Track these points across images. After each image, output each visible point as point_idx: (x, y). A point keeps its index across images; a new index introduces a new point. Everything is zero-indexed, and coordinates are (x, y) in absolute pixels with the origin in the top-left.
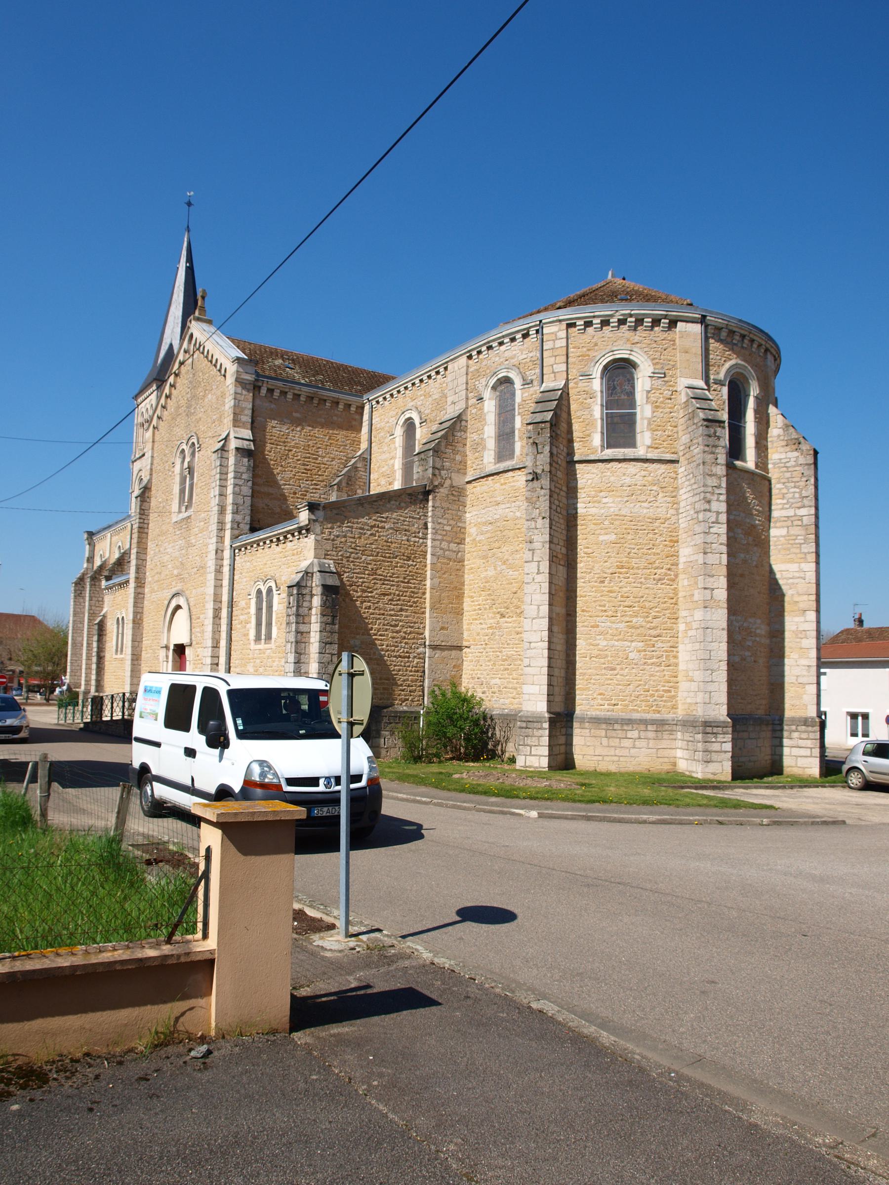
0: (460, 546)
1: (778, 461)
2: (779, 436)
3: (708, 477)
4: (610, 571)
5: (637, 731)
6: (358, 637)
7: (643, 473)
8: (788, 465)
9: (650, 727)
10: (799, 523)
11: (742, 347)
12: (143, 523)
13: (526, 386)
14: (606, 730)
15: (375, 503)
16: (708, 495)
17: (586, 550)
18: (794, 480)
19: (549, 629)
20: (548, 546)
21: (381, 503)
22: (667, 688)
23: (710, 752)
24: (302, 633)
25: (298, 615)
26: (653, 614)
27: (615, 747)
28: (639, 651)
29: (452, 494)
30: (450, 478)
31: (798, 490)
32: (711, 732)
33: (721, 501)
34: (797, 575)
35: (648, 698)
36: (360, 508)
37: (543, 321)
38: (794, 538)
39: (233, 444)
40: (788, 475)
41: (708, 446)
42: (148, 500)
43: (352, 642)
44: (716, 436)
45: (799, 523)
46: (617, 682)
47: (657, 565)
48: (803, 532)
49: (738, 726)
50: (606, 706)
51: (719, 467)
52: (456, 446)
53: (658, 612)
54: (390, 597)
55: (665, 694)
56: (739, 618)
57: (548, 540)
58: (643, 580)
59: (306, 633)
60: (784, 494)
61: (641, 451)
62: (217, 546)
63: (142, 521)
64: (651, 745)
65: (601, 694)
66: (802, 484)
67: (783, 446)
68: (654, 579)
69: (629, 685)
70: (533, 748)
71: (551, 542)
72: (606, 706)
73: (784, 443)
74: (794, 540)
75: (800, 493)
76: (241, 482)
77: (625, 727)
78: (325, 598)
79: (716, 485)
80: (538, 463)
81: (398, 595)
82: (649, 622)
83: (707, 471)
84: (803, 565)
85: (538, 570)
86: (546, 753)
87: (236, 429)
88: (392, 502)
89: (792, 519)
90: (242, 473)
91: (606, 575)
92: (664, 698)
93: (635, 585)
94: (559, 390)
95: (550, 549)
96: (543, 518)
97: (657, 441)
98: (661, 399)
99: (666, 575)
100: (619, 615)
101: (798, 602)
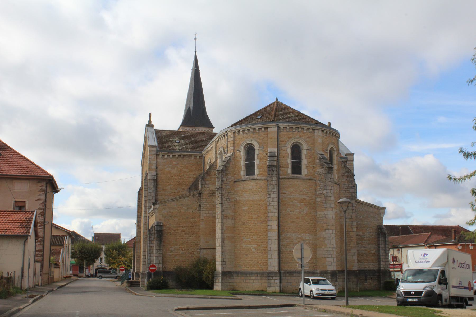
0: (214, 212)
1: (318, 172)
2: (318, 162)
4: (246, 220)
5: (254, 277)
6: (173, 247)
8: (321, 174)
9: (259, 275)
10: (323, 196)
11: (298, 132)
12: (140, 203)
13: (225, 155)
14: (245, 277)
15: (179, 200)
16: (270, 192)
17: (239, 213)
18: (322, 179)
19: (222, 242)
20: (221, 213)
21: (181, 199)
22: (265, 261)
23: (271, 283)
24: (151, 247)
25: (150, 241)
26: (260, 235)
27: (248, 283)
28: (255, 248)
29: (210, 193)
30: (209, 188)
31: (323, 183)
32: (270, 276)
33: (275, 194)
34: (323, 216)
35: (259, 265)
36: (173, 202)
37: (227, 131)
38: (322, 202)
40: (320, 177)
41: (269, 175)
43: (170, 249)
44: (272, 171)
45: (323, 196)
46: (248, 260)
47: (261, 217)
48: (325, 200)
49: (295, 275)
50: (245, 268)
51: (274, 182)
52: (211, 176)
53: (261, 234)
54: (185, 232)
55: (265, 263)
57: (221, 211)
58: (256, 223)
59: (153, 246)
60: (320, 185)
61: (255, 177)
62: (144, 215)
63: (139, 202)
64: (259, 282)
65: (244, 264)
66: (324, 181)
67: (319, 166)
68: (260, 222)
69: (252, 260)
70: (218, 283)
71: (222, 212)
72: (245, 268)
73: (319, 165)
74: (322, 202)
75: (324, 184)
76: (151, 191)
77: (251, 276)
78: (157, 234)
79: (272, 188)
80: (219, 185)
81: (189, 231)
82: (258, 238)
83: (269, 183)
84: (325, 212)
85: (219, 222)
86: (220, 285)
87: (149, 172)
88: (185, 199)
89: (322, 194)
90: (151, 188)
91: (245, 222)
93: (254, 225)
94: (229, 157)
95: (222, 214)
96: (220, 204)
97: (261, 172)
98: (262, 157)
99: (264, 220)
100: (249, 236)
101: (324, 226)
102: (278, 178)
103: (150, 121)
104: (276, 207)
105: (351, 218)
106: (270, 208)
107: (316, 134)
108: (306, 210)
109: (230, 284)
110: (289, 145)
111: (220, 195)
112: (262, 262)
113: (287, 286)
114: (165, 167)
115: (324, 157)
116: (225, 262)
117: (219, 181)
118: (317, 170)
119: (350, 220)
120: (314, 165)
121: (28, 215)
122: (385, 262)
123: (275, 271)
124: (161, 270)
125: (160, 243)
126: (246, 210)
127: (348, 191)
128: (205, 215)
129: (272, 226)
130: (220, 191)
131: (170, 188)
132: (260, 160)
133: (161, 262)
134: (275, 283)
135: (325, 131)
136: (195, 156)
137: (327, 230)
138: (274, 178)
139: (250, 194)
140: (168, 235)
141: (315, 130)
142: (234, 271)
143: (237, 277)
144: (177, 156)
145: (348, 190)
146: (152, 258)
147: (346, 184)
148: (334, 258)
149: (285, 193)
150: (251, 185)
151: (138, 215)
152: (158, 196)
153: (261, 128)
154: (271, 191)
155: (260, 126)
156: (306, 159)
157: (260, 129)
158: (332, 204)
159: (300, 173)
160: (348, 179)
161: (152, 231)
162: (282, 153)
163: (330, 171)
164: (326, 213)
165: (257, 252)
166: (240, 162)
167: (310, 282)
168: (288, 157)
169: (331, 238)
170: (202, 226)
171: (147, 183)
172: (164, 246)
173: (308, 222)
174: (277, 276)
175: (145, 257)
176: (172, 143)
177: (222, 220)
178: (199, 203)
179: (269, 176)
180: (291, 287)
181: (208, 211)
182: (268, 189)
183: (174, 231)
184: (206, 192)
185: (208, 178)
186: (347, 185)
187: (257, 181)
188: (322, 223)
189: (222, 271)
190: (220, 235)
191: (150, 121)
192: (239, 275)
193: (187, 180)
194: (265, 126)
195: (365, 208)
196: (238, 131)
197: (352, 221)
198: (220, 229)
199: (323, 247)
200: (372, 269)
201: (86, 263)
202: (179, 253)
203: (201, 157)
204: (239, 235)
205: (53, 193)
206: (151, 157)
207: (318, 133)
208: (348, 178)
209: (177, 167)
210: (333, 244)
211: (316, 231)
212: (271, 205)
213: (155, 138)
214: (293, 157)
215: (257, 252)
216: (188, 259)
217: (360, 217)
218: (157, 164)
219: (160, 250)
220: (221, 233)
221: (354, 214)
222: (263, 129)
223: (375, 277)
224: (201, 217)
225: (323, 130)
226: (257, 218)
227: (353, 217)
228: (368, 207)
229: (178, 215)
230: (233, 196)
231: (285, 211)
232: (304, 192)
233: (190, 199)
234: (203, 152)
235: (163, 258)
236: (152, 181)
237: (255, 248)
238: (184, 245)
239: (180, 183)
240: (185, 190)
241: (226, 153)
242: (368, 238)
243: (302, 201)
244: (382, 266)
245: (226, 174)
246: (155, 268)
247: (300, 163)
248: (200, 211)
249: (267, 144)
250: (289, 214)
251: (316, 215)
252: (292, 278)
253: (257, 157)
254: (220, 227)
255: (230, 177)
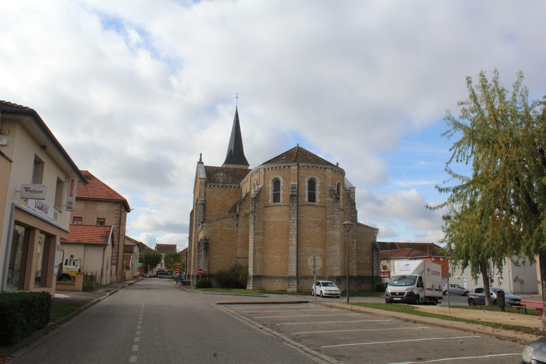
3: (291, 211)
7: (280, 209)
9: (281, 279)
10: (332, 219)
11: (314, 170)
16: (291, 216)
19: (254, 253)
21: (223, 220)
23: (290, 285)
24: (200, 255)
25: (198, 251)
28: (279, 258)
36: (217, 222)
39: (199, 202)
40: (330, 205)
42: (193, 215)
43: (214, 257)
45: (332, 219)
49: (309, 279)
51: (294, 207)
56: (310, 248)
58: (280, 239)
60: (329, 210)
61: (280, 203)
65: (270, 270)
71: (254, 230)
73: (329, 196)
76: (200, 213)
77: (275, 279)
88: (226, 219)
90: (200, 210)
92: (286, 271)
94: (260, 188)
95: (254, 232)
99: (286, 237)
102: (298, 205)
103: (201, 159)
104: (296, 227)
105: (353, 237)
106: (291, 227)
107: (327, 172)
108: (318, 229)
109: (260, 285)
110: (306, 180)
111: (253, 217)
112: (284, 269)
113: (303, 288)
114: (212, 195)
115: (333, 189)
116: (256, 268)
117: (252, 206)
118: (328, 200)
119: (352, 238)
120: (325, 196)
121: (107, 229)
122: (377, 270)
123: (294, 276)
124: (207, 273)
125: (207, 253)
126: (273, 229)
127: (351, 216)
128: (241, 232)
129: (293, 242)
130: (253, 214)
131: (215, 211)
132: (284, 191)
133: (207, 267)
134: (293, 285)
135: (334, 170)
136: (235, 187)
137: (334, 246)
138: (294, 205)
139: (276, 217)
140: (213, 246)
141: (327, 169)
142: (262, 275)
143: (265, 280)
144: (220, 186)
145: (350, 215)
146: (200, 264)
147: (349, 210)
148: (339, 266)
149: (303, 217)
150: (277, 210)
151: (190, 231)
152: (205, 216)
153: (285, 166)
154: (292, 215)
155: (284, 165)
156: (319, 190)
157: (284, 167)
158: (338, 225)
159: (314, 201)
160: (351, 206)
161: (201, 243)
162: (301, 185)
163: (337, 200)
164: (333, 232)
165: (281, 261)
166: (268, 192)
167: (320, 285)
168: (306, 189)
169: (337, 251)
170: (239, 240)
171: (198, 206)
172: (209, 255)
173: (320, 239)
174: (295, 280)
175: (194, 263)
176: (217, 176)
177: (254, 236)
178: (237, 223)
179: (291, 203)
180: (306, 288)
181: (243, 229)
182: (290, 213)
183: (218, 243)
184: (242, 215)
185: (244, 204)
186: (350, 211)
187: (281, 207)
188: (330, 239)
189: (253, 275)
190: (253, 247)
191: (201, 159)
192: (267, 278)
193: (228, 205)
194: (289, 164)
195: (363, 229)
196: (268, 168)
197: (353, 239)
198: (253, 243)
199: (331, 258)
200: (368, 275)
201: (150, 266)
202: (221, 260)
203: (239, 188)
204: (267, 247)
205: (126, 213)
206: (201, 187)
207: (329, 171)
208: (350, 206)
209: (221, 195)
210: (338, 256)
211: (325, 246)
212: (292, 225)
213: (205, 172)
214: (310, 189)
215: (281, 261)
216: (228, 266)
217: (359, 235)
218: (205, 192)
219: (206, 258)
220: (253, 246)
221: (355, 233)
222: (287, 167)
223: (369, 281)
224: (238, 233)
225: (332, 169)
226: (281, 235)
227: (354, 236)
228: (366, 228)
229: (221, 231)
230: (263, 218)
231: (302, 230)
232: (317, 216)
233: (230, 219)
234: (241, 184)
235: (208, 264)
236: (201, 205)
237: (279, 258)
238: (225, 255)
239: (223, 207)
240: (226, 212)
241: (258, 185)
242: (365, 252)
243: (315, 223)
244: (375, 273)
245: (258, 201)
246: (202, 272)
247: (314, 194)
248: (237, 229)
249: (290, 179)
250: (306, 233)
251: (326, 234)
252: (306, 281)
253: (282, 188)
254: (253, 241)
255: (261, 203)
